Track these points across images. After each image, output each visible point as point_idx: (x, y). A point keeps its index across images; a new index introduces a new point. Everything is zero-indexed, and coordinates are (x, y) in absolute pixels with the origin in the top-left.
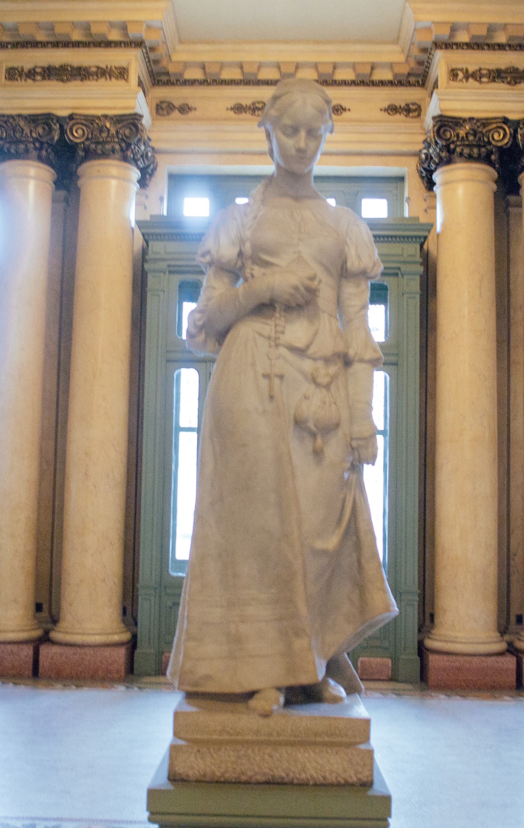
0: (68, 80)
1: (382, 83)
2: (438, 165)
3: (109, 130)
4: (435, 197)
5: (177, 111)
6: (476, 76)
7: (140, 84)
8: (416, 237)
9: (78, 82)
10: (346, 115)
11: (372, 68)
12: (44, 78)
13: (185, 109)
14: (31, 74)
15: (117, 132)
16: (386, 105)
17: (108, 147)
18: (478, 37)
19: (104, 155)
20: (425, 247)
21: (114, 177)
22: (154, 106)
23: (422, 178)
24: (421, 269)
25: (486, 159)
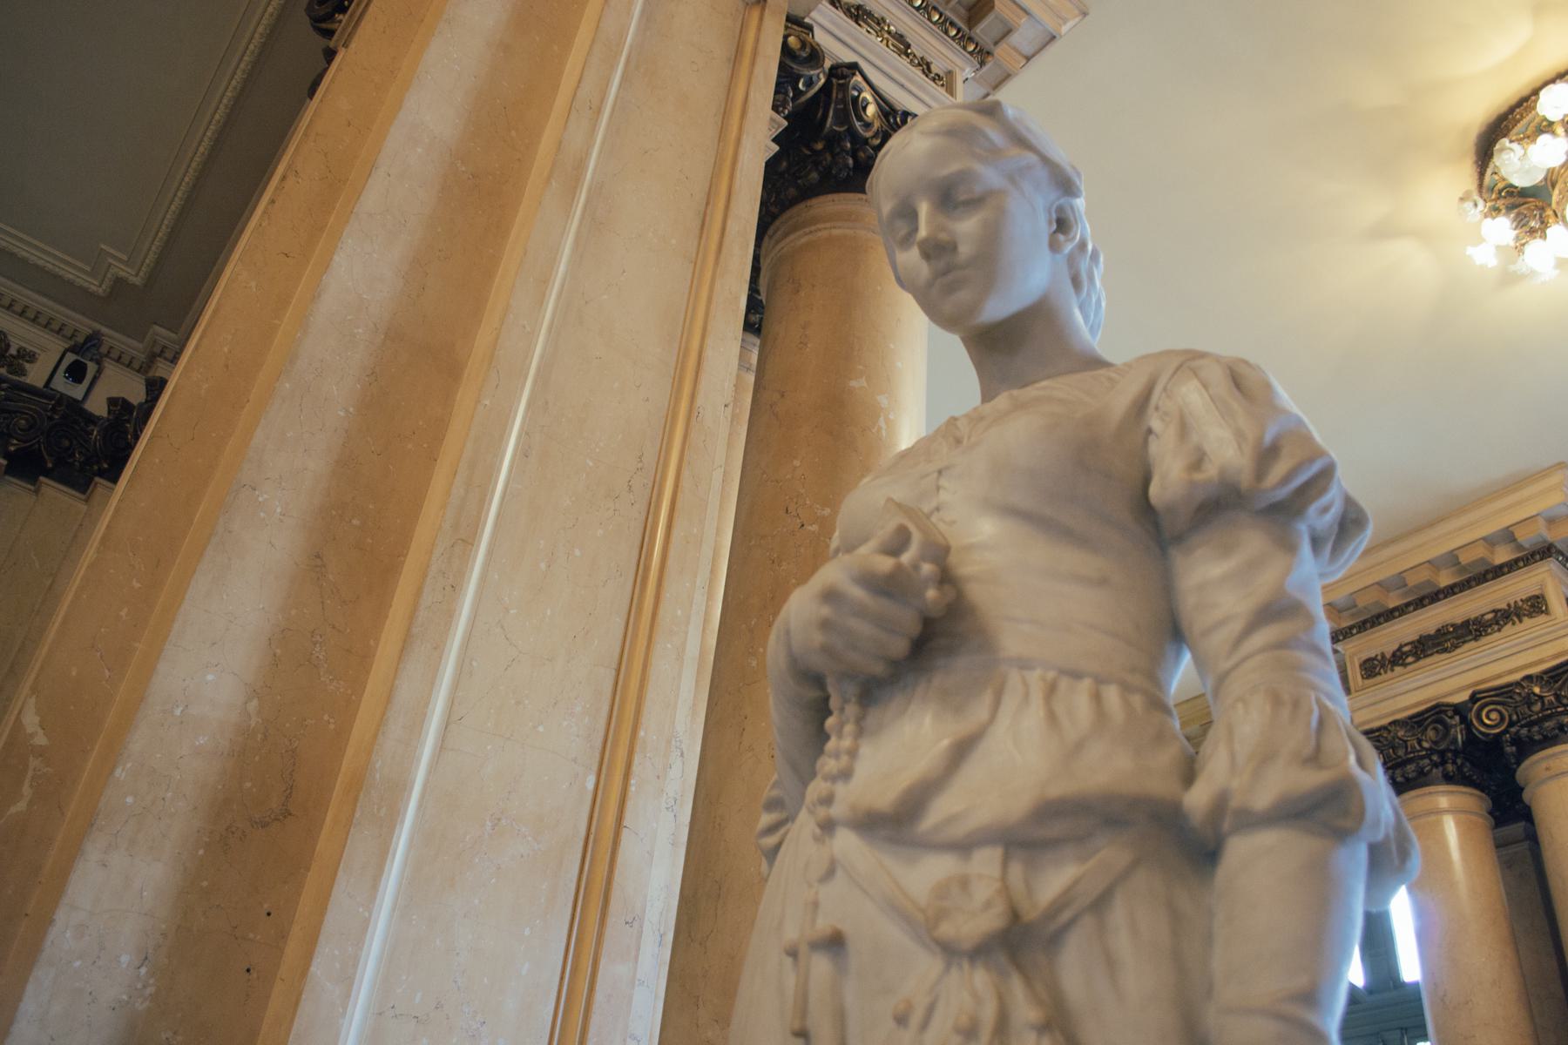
0: (1456, 647)
3: (1541, 698)
9: (1473, 644)
12: (1418, 659)
14: (1398, 659)
15: (1557, 697)
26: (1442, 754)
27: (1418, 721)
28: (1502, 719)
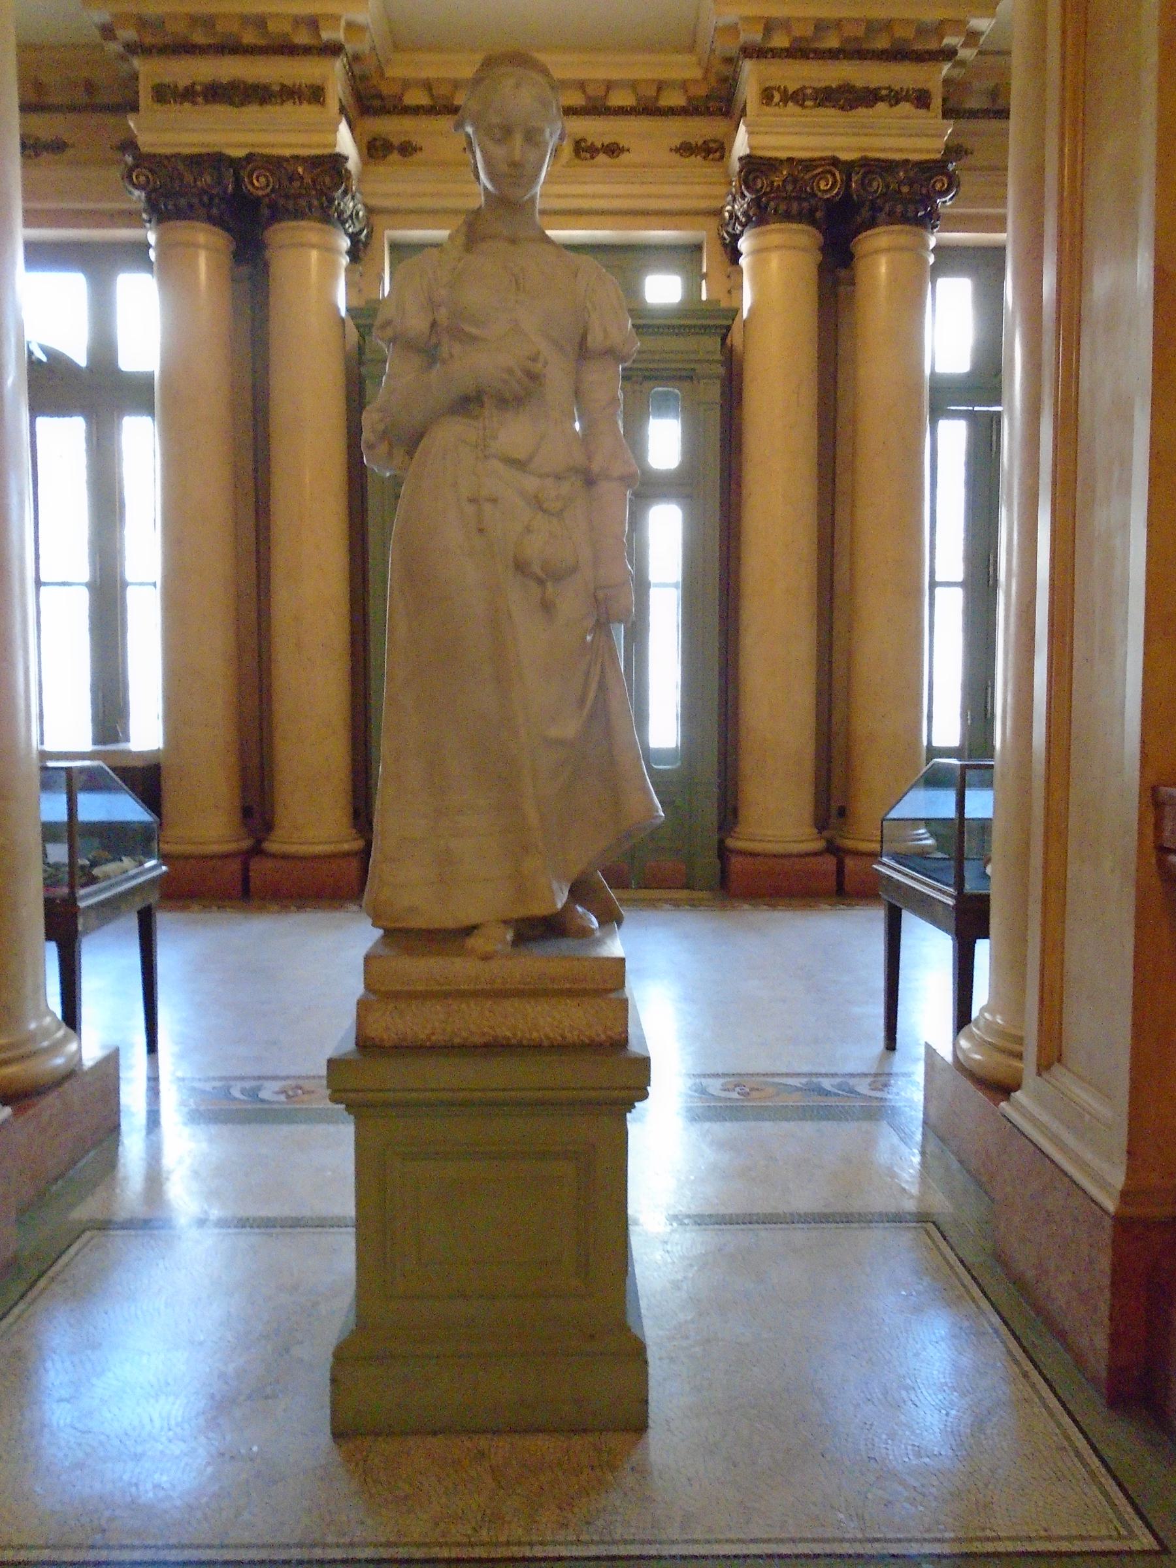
1: (672, 112)
2: (744, 226)
3: (302, 178)
4: (740, 272)
5: (396, 152)
6: (797, 97)
7: (342, 110)
8: (716, 327)
10: (625, 157)
11: (659, 89)
12: (207, 101)
13: (407, 149)
14: (188, 95)
15: (314, 181)
16: (677, 142)
17: (303, 202)
18: (801, 39)
19: (299, 215)
20: (728, 341)
21: (313, 246)
22: (365, 141)
23: (725, 245)
24: (721, 370)
25: (807, 217)
26: (211, 198)
27: (196, 161)
28: (268, 185)
